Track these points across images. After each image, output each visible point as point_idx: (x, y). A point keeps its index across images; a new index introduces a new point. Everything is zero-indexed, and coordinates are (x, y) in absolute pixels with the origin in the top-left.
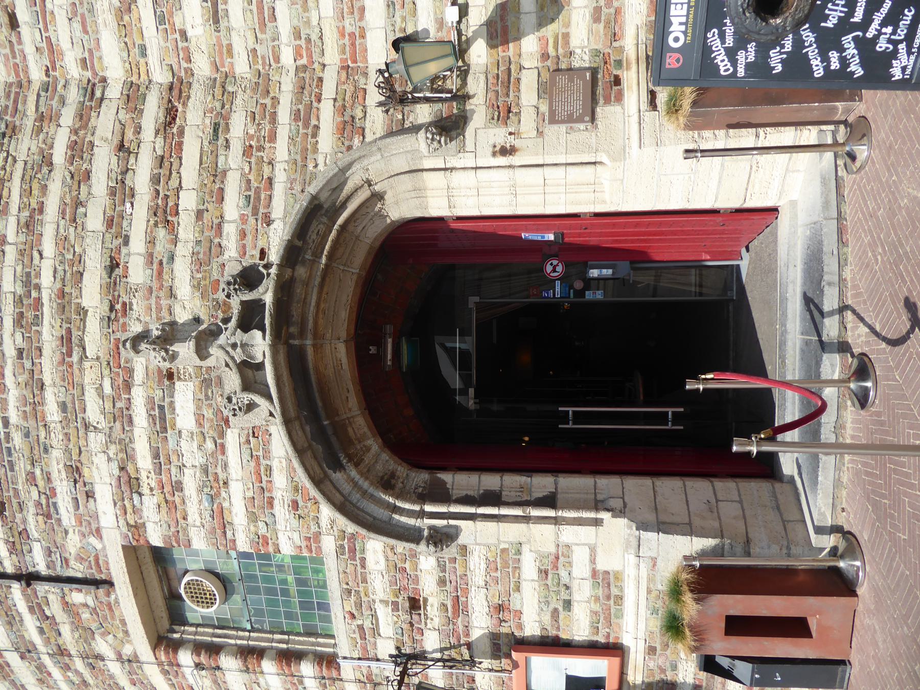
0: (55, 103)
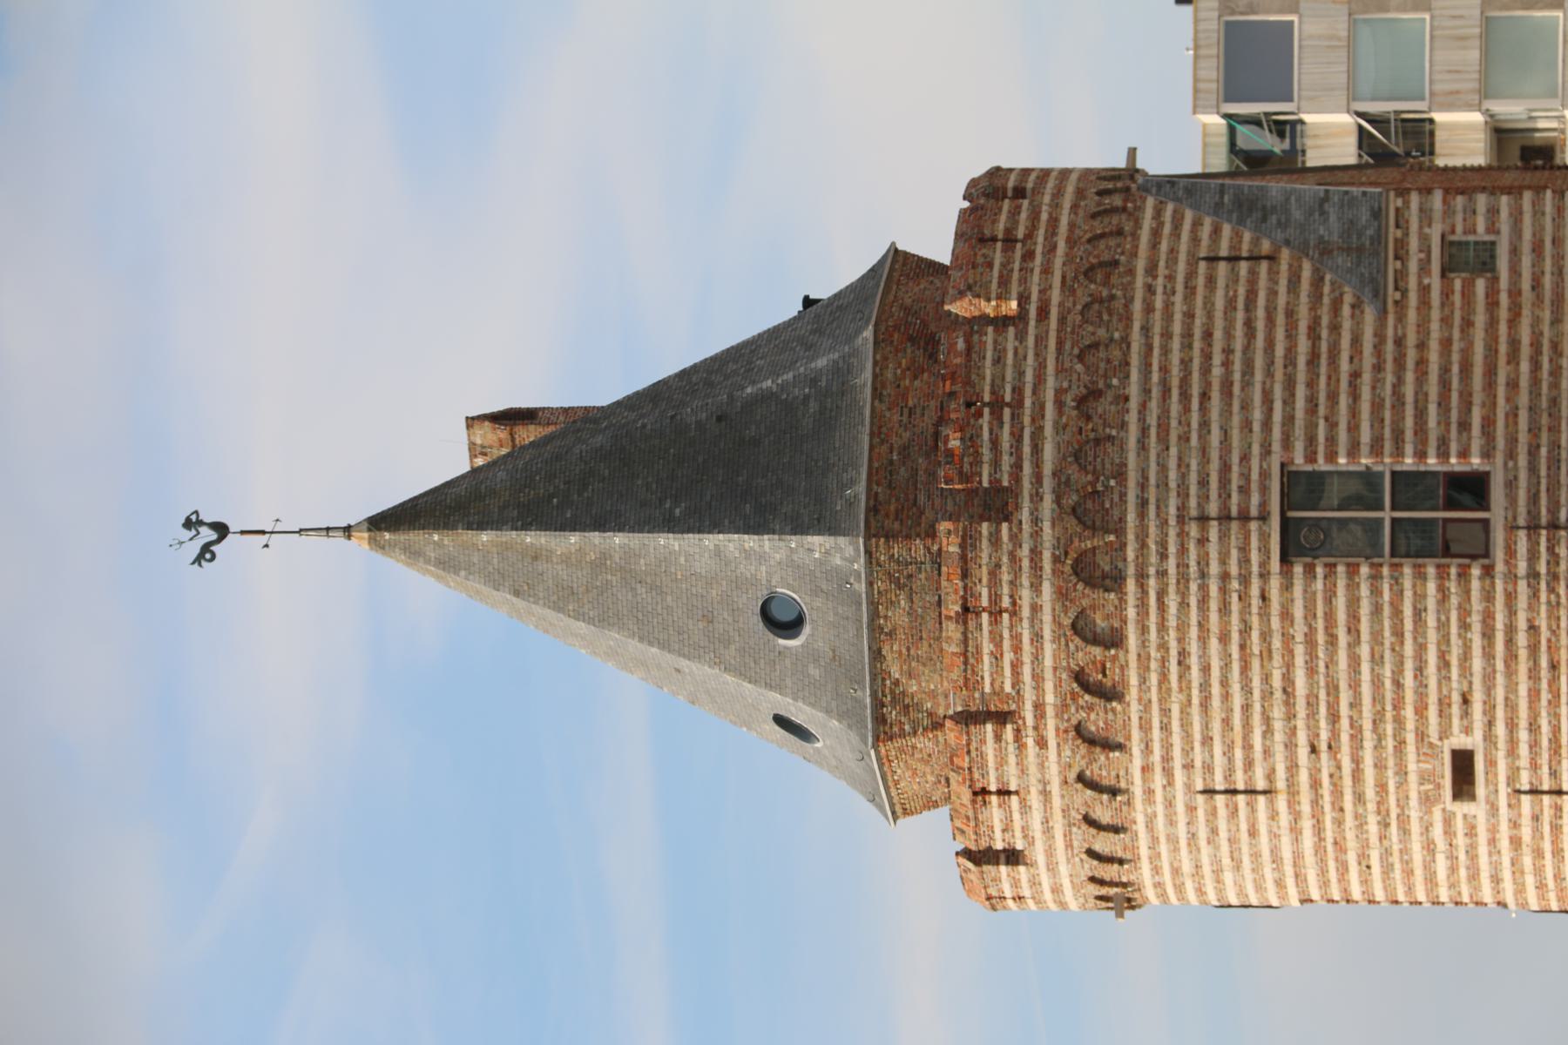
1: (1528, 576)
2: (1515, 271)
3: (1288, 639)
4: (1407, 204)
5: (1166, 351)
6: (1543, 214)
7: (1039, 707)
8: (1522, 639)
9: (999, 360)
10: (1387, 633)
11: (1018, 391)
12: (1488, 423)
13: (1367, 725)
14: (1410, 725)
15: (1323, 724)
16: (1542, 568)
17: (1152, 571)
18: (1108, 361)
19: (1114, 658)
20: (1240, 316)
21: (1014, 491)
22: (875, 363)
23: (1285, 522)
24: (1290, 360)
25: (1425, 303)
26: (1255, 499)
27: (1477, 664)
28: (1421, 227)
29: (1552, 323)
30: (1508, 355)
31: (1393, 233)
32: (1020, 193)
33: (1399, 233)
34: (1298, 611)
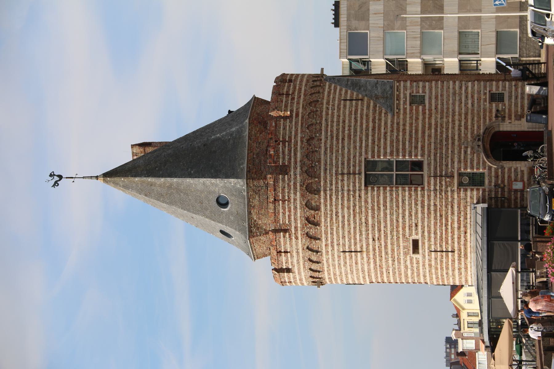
1: (434, 190)
2: (430, 104)
3: (366, 208)
5: (332, 126)
7: (296, 228)
8: (432, 208)
9: (284, 129)
10: (394, 207)
11: (290, 137)
12: (423, 147)
13: (389, 233)
14: (401, 233)
15: (376, 232)
16: (438, 188)
17: (328, 189)
18: (316, 129)
19: (317, 214)
20: (353, 116)
21: (289, 166)
22: (249, 129)
23: (366, 175)
24: (367, 129)
25: (405, 113)
26: (357, 168)
27: (420, 215)
29: (441, 119)
31: (396, 93)
32: (290, 81)
33: (398, 93)
34: (369, 200)
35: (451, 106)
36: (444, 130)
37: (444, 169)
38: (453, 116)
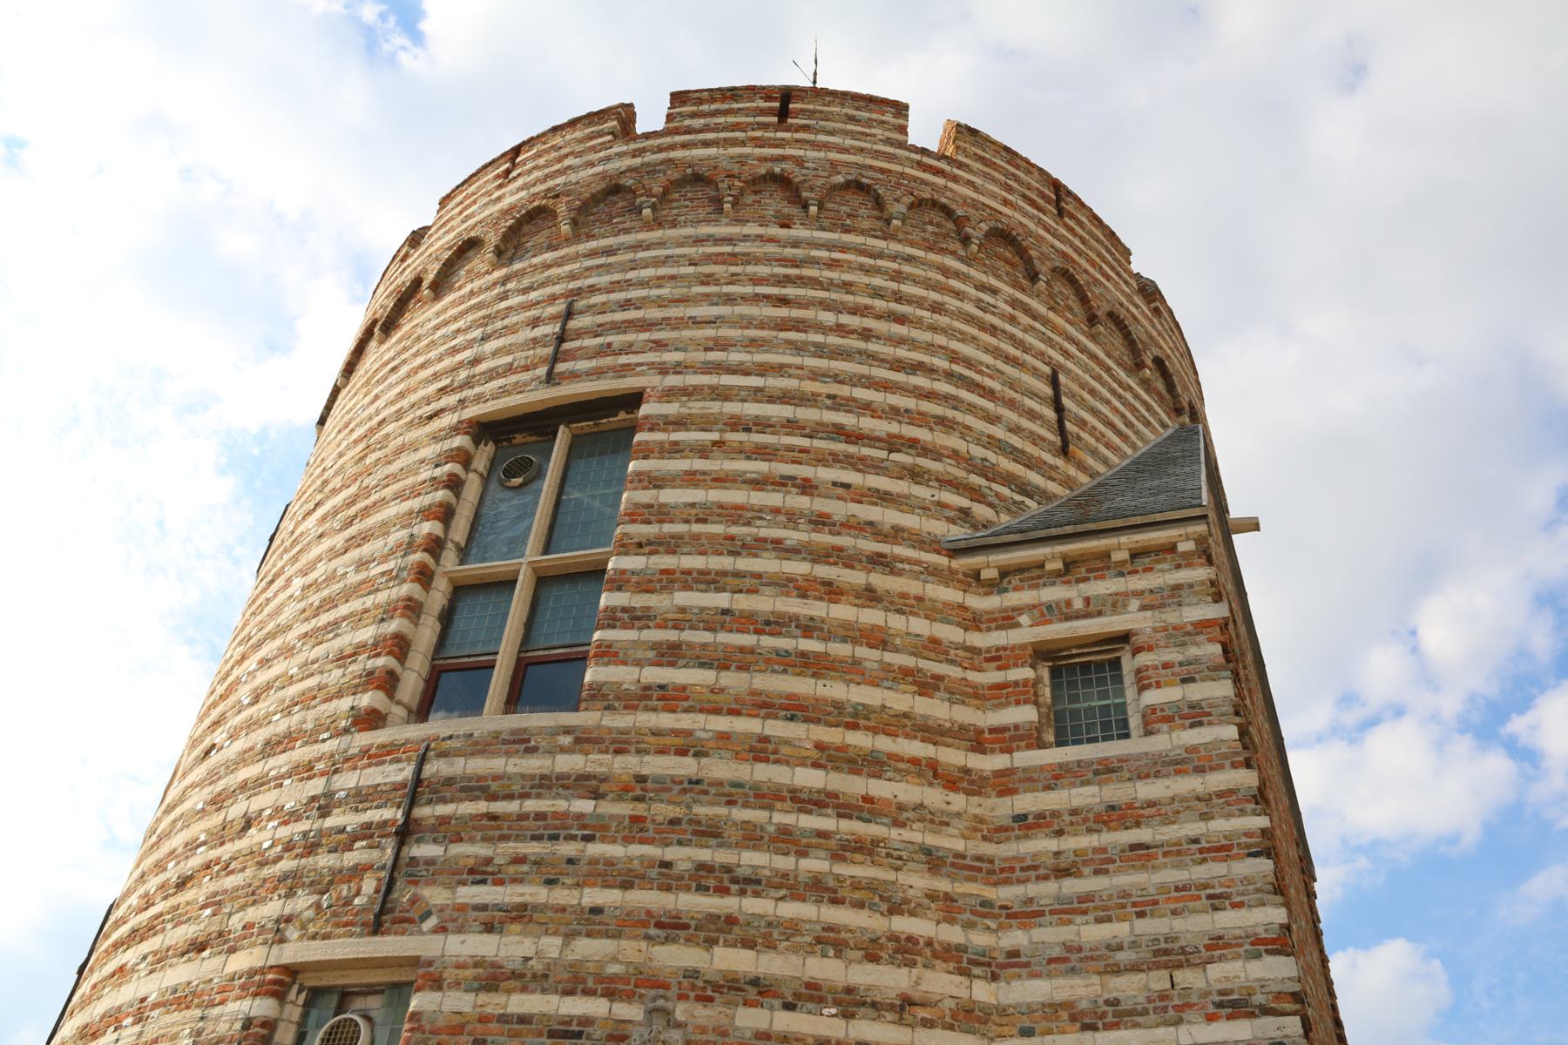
0: (967, 916)
2: (1057, 777)
4: (1186, 561)
6: (1205, 817)
12: (670, 698)
20: (941, 363)
28: (1138, 594)
29: (927, 851)
30: (844, 748)
35: (1050, 935)
36: (816, 864)
37: (456, 849)
38: (962, 961)
